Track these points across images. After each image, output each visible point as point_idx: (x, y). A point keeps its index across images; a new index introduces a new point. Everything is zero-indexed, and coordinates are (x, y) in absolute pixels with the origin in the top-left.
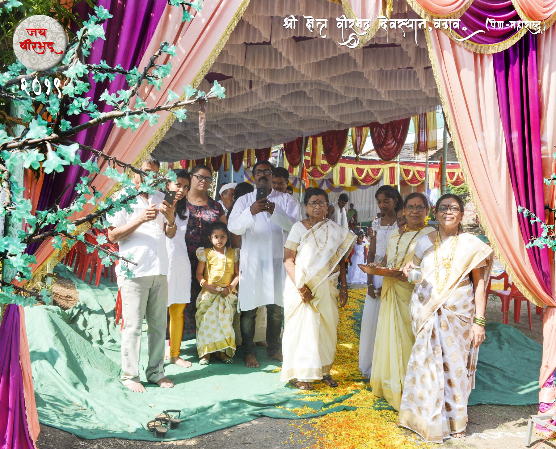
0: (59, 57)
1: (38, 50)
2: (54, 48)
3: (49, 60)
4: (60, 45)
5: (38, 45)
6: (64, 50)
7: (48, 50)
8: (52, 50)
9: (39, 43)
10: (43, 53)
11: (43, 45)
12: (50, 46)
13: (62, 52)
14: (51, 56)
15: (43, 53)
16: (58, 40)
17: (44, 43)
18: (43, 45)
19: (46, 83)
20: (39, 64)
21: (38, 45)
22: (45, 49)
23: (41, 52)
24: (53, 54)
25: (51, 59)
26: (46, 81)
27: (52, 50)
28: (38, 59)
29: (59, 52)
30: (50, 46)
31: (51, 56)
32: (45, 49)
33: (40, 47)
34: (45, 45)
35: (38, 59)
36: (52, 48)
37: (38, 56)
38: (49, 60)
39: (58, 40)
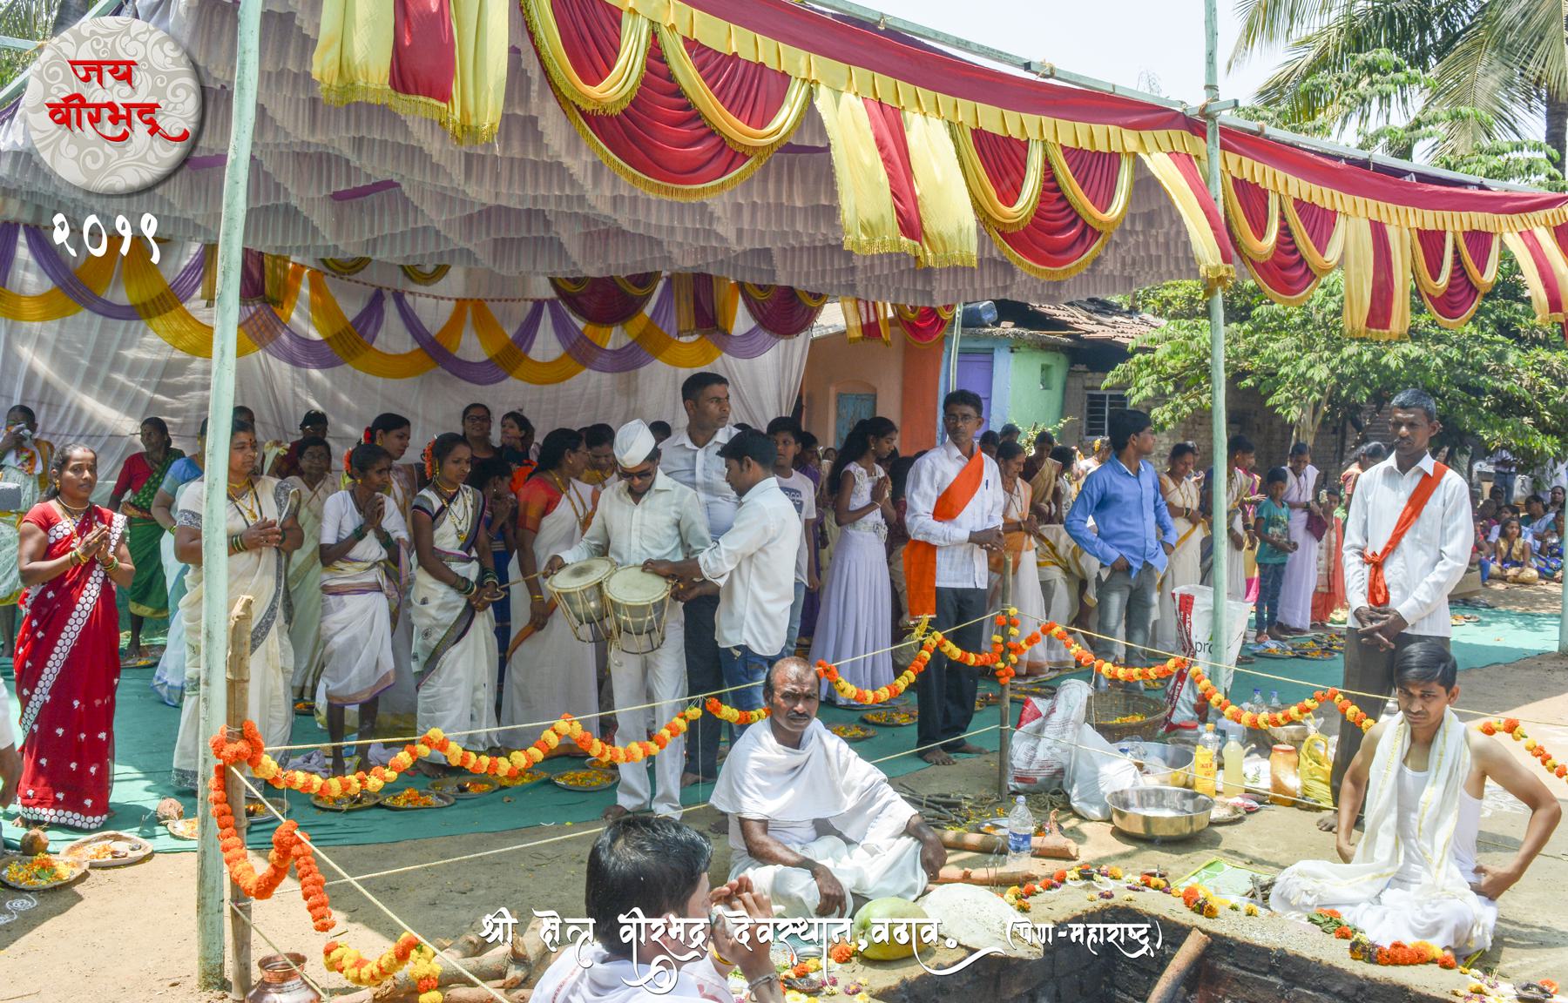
0: (175, 151)
1: (108, 128)
2: (161, 121)
3: (143, 159)
4: (180, 113)
5: (106, 113)
6: (190, 127)
7: (140, 129)
8: (154, 129)
9: (111, 106)
10: (125, 136)
11: (123, 112)
12: (146, 117)
13: (185, 135)
14: (151, 147)
15: (125, 136)
16: (174, 94)
17: (128, 106)
18: (123, 112)
19: (118, 227)
20: (112, 174)
21: (106, 113)
22: (129, 124)
23: (119, 133)
24: (158, 141)
25: (151, 157)
26: (121, 220)
27: (154, 129)
28: (108, 157)
29: (176, 133)
30: (146, 117)
31: (151, 147)
32: (129, 124)
33: (115, 120)
34: (129, 113)
35: (108, 157)
36: (151, 122)
37: (108, 147)
38: (143, 159)
39: (174, 94)
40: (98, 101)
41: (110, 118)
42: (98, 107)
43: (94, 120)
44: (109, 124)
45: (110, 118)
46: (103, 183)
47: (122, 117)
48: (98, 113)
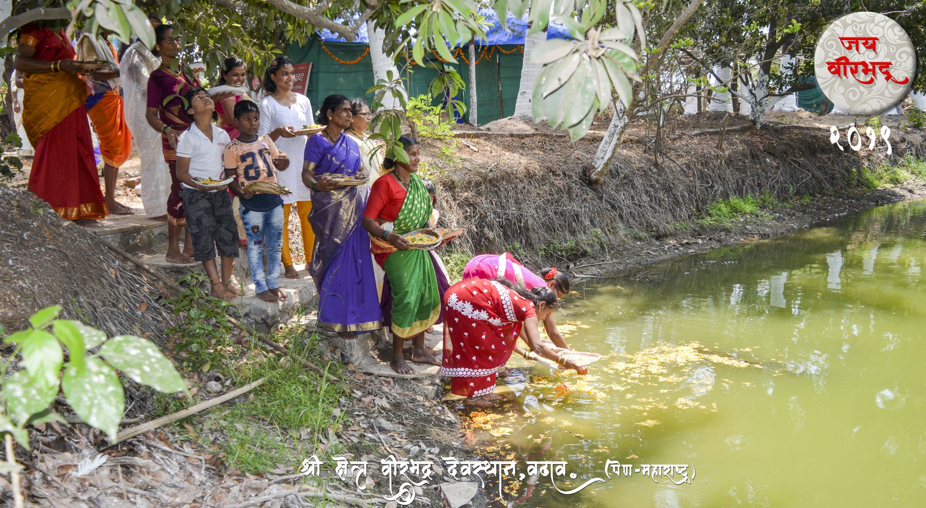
1: (862, 77)
5: (861, 68)
9: (864, 63)
10: (872, 81)
11: (870, 67)
15: (872, 81)
17: (872, 63)
18: (870, 67)
20: (865, 102)
21: (861, 68)
23: (868, 79)
28: (862, 93)
33: (866, 71)
35: (862, 93)
37: (862, 88)
40: (856, 61)
41: (863, 71)
42: (856, 64)
43: (854, 72)
44: (863, 74)
45: (863, 71)
46: (859, 108)
47: (870, 70)
48: (856, 68)
